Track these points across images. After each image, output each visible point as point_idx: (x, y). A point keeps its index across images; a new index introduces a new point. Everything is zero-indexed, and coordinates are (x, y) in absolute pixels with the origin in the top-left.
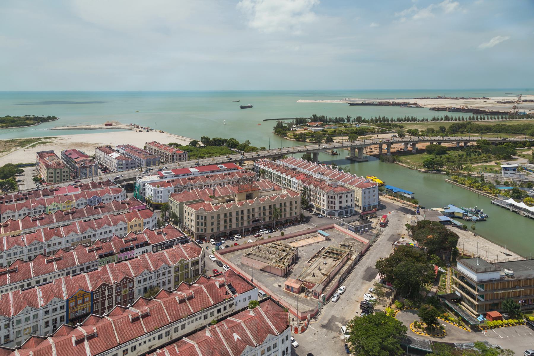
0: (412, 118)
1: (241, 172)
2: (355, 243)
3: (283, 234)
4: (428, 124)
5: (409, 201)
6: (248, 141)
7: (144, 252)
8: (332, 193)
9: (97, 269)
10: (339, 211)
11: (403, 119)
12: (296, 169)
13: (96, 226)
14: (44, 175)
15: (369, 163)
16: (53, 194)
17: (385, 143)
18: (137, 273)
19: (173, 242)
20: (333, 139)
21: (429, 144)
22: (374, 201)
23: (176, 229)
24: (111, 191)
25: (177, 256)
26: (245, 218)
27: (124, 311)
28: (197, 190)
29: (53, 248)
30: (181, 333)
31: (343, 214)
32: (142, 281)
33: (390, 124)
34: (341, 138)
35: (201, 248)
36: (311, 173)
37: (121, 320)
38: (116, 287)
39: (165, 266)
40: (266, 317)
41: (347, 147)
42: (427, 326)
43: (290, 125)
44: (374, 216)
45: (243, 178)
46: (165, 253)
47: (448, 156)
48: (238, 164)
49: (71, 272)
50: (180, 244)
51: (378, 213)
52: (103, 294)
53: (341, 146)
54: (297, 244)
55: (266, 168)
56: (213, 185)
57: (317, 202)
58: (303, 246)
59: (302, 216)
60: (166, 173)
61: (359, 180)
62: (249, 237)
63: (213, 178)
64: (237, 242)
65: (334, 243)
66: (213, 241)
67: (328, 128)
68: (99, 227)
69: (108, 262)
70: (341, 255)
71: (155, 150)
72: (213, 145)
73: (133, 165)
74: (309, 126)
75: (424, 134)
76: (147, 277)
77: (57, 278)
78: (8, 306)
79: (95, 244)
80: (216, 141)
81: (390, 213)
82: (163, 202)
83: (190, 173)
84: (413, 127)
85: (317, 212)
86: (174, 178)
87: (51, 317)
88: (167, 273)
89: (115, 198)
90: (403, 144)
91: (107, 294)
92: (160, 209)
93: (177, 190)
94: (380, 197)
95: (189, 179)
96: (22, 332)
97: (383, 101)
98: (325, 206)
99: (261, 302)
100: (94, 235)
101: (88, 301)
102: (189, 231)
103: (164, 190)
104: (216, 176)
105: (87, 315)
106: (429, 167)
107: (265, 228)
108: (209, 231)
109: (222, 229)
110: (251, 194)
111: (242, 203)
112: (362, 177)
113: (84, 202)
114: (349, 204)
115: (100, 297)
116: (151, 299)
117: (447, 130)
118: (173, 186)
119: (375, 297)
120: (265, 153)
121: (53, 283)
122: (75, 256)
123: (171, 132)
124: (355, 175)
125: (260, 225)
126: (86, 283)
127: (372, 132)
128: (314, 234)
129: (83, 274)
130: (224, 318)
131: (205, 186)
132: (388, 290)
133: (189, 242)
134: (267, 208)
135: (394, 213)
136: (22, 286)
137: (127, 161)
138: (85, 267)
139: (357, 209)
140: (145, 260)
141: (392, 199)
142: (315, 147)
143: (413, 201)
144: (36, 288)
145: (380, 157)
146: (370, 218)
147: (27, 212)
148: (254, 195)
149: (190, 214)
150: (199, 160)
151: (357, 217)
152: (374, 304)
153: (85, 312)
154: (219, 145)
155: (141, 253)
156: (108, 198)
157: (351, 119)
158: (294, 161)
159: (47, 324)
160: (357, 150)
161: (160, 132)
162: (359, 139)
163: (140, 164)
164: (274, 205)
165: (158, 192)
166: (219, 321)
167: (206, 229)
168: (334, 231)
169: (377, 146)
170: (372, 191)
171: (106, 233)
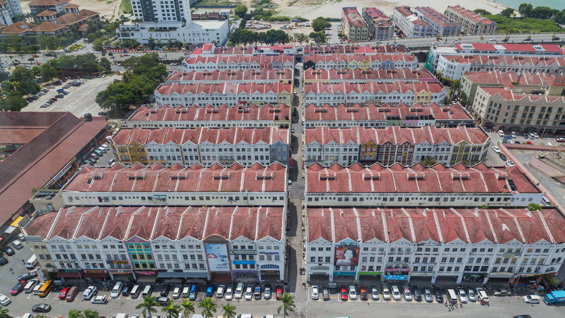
7: (427, 125)
9: (384, 128)
13: (387, 89)
16: (354, 52)
18: (418, 141)
19: (458, 122)
23: (464, 110)
25: (459, 137)
27: (403, 169)
28: (498, 73)
29: (351, 101)
32: (421, 150)
35: (488, 136)
37: (400, 175)
38: (399, 147)
39: (446, 143)
46: (448, 131)
49: (364, 125)
50: (465, 127)
52: (387, 150)
56: (520, 70)
60: (465, 47)
63: (523, 61)
66: (502, 133)
68: (390, 91)
69: (394, 125)
73: (429, 33)
76: (427, 147)
77: (353, 126)
78: (321, 136)
79: (385, 106)
82: (454, 79)
83: (495, 51)
87: (348, 154)
88: (445, 150)
89: (406, 65)
91: (390, 151)
92: (450, 86)
93: (473, 69)
95: (491, 58)
96: (329, 157)
100: (384, 98)
103: (459, 66)
104: (528, 60)
105: (373, 162)
111: (554, 99)
113: (378, 64)
116: (428, 168)
118: (470, 63)
121: (351, 129)
126: (375, 136)
129: (373, 129)
131: (509, 69)
133: (475, 127)
136: (329, 125)
138: (375, 123)
140: (427, 132)
144: (339, 129)
147: (333, 65)
149: (482, 98)
150: (510, 36)
153: (371, 159)
155: (424, 125)
156: (401, 64)
159: (345, 158)
163: (438, 32)
171: (394, 98)
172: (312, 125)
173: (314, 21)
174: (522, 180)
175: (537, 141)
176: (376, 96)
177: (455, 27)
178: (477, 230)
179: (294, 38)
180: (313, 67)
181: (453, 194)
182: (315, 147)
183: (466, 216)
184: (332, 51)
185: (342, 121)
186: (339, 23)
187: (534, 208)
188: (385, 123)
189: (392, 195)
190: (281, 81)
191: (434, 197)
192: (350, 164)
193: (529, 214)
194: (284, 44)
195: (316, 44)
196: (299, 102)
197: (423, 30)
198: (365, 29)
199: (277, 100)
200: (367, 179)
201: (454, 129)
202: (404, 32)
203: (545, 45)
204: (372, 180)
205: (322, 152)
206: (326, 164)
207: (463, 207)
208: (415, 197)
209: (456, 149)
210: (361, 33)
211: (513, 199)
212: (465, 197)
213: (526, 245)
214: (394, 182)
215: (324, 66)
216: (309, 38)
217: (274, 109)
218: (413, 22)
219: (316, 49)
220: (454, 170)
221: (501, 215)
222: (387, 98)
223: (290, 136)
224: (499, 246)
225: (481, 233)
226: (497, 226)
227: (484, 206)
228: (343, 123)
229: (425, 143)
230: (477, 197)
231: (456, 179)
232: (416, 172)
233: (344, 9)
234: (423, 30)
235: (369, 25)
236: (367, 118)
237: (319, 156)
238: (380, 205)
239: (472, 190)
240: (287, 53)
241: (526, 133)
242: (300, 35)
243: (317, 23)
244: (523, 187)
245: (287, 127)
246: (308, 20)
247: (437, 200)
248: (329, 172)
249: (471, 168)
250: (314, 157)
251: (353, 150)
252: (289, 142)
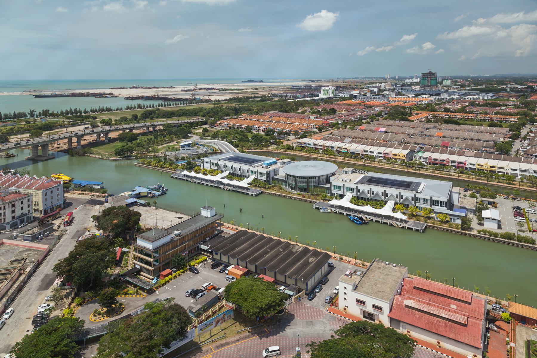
0: (106, 108)
2: (31, 253)
4: (122, 113)
5: (98, 192)
10: (11, 223)
11: (98, 109)
15: (57, 160)
20: (8, 139)
21: (121, 132)
22: (58, 200)
31: (17, 225)
33: (83, 116)
34: (19, 136)
44: (57, 216)
47: (138, 141)
51: (62, 212)
70: (9, 274)
75: (118, 122)
81: (76, 209)
84: (106, 117)
90: (96, 135)
94: (66, 195)
106: (120, 155)
112: (44, 177)
114: (25, 211)
117: (139, 118)
124: (35, 176)
127: (62, 126)
135: (81, 208)
141: (80, 194)
143: (102, 191)
145: (70, 152)
146: (52, 221)
151: (36, 223)
160: (40, 148)
162: (44, 134)
169: (66, 140)
170: (55, 190)
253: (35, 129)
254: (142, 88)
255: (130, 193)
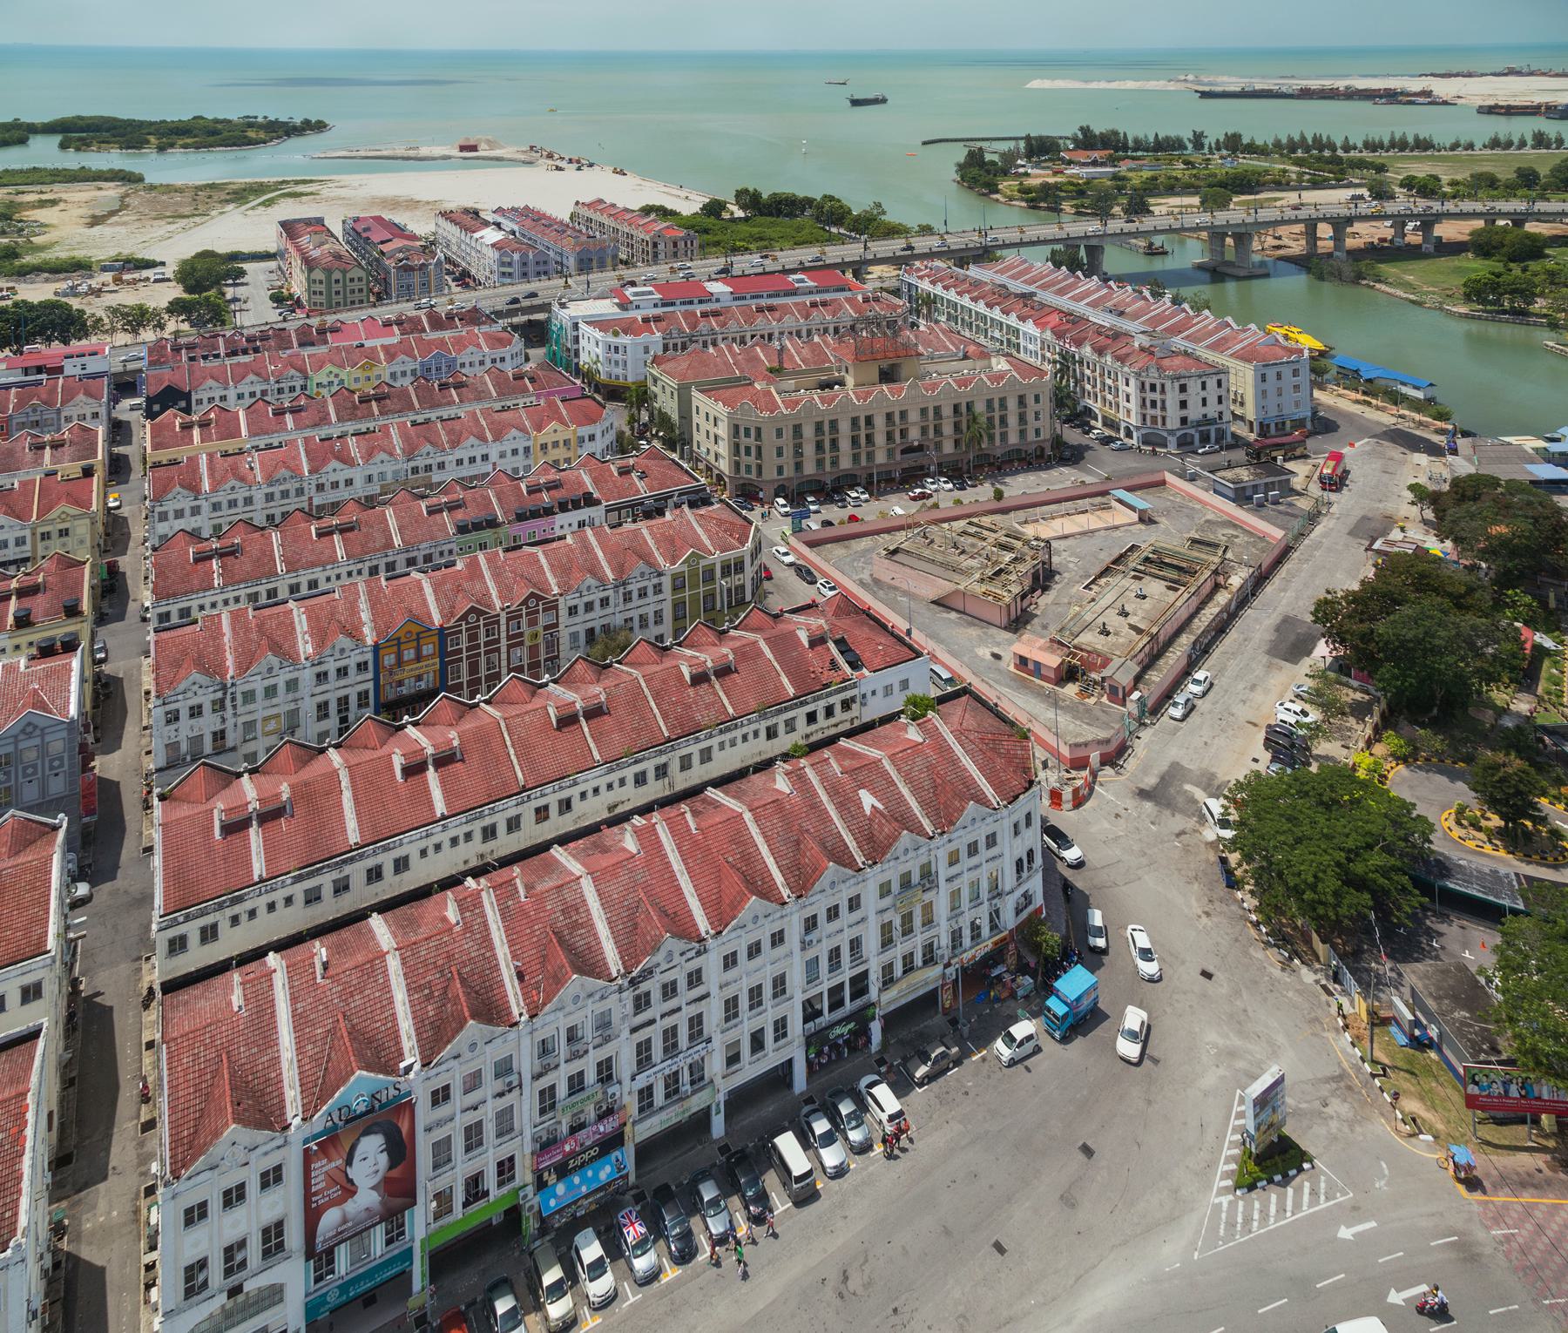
1: (860, 298)
3: (999, 495)
5: (1418, 410)
6: (879, 205)
7: (581, 524)
8: (1153, 377)
9: (453, 564)
10: (1179, 433)
11: (1386, 142)
12: (1033, 294)
13: (444, 438)
14: (298, 286)
16: (326, 342)
17: (1325, 219)
18: (566, 583)
19: (666, 499)
22: (1297, 404)
24: (481, 341)
25: (678, 543)
26: (880, 439)
27: (533, 694)
28: (730, 349)
29: (331, 496)
30: (698, 773)
31: (1192, 443)
32: (581, 609)
34: (1175, 201)
35: (751, 523)
36: (1081, 308)
37: (527, 718)
38: (509, 620)
39: (647, 570)
40: (958, 750)
41: (1198, 228)
42: (1502, 823)
43: (1009, 158)
44: (1298, 452)
45: (867, 318)
46: (645, 532)
47: (1550, 264)
48: (849, 275)
49: (382, 568)
50: (685, 507)
51: (1311, 443)
52: (473, 637)
53: (1177, 225)
54: (1047, 530)
55: (938, 290)
57: (1104, 399)
58: (1065, 537)
59: (1058, 442)
60: (636, 294)
61: (1242, 336)
62: (893, 498)
63: (777, 315)
64: (857, 512)
65: (1167, 532)
67: (1130, 170)
68: (455, 444)
69: (483, 547)
70: (1193, 573)
71: (602, 225)
72: (771, 214)
74: (1070, 163)
75: (1461, 191)
76: (596, 597)
77: (345, 581)
78: (219, 650)
79: (444, 492)
80: (780, 202)
81: (1352, 445)
82: (630, 379)
83: (708, 298)
84: (1421, 170)
85: (1108, 432)
86: (659, 311)
87: (333, 691)
88: (650, 591)
89: (494, 361)
90: (1388, 223)
91: (482, 639)
92: (623, 400)
94: (1317, 393)
95: (705, 315)
96: (259, 725)
97: (1314, 84)
98: (1133, 414)
99: (942, 700)
100: (441, 466)
101: (432, 656)
102: (709, 469)
104: (785, 309)
105: (432, 694)
106: (1484, 302)
107: (941, 474)
108: (770, 474)
109: (809, 469)
110: (894, 367)
111: (869, 394)
112: (1253, 326)
113: (409, 367)
114: (1212, 410)
115: (464, 646)
116: (610, 666)
119: (1314, 716)
120: (933, 243)
121: (337, 596)
122: (392, 523)
123: (649, 172)
124: (1229, 319)
125: (925, 462)
126: (425, 601)
127: (1281, 184)
128: (1098, 500)
129: (415, 575)
130: (831, 741)
132: (1358, 696)
134: (947, 411)
135: (1368, 448)
136: (253, 597)
137: (524, 255)
138: (420, 556)
139: (1240, 429)
141: (1357, 402)
142: (1092, 226)
143: (1433, 411)
144: (291, 604)
145: (1307, 263)
147: (258, 389)
148: (904, 372)
151: (1239, 455)
152: (1310, 738)
153: (423, 685)
154: (791, 215)
156: (476, 359)
157: (1206, 142)
158: (1027, 271)
160: (1229, 241)
161: (615, 171)
164: (969, 406)
165: (616, 348)
166: (814, 747)
167: (759, 467)
168: (1165, 495)
169: (1299, 228)
170: (1287, 372)
171: (472, 460)
172: (185, 613)
173: (184, 263)
174: (866, 629)
175: (871, 510)
176: (412, 464)
177: (603, 249)
178: (798, 843)
179: (106, 321)
180: (183, 404)
181: (701, 735)
182: (195, 701)
183: (756, 804)
184: (252, 345)
185: (302, 572)
186: (272, 265)
187: (918, 709)
188: (453, 546)
189: (509, 808)
190: (51, 474)
191: (649, 766)
192: (347, 728)
193: (913, 734)
194: (66, 342)
195: (194, 331)
196: (129, 535)
197: (525, 264)
198: (356, 273)
199: (28, 547)
200: (414, 770)
201: (658, 521)
202: (473, 272)
203: (812, 273)
204: (431, 768)
205: (230, 711)
206: (250, 758)
207: (741, 774)
208: (588, 787)
209: (678, 583)
210: (345, 286)
211: (864, 696)
212: (738, 733)
213: (938, 841)
214: (512, 752)
215: (223, 398)
216: (166, 317)
217: (14, 584)
218: (493, 245)
219: (190, 347)
220: (688, 652)
221: (847, 763)
222: (450, 467)
223: (83, 680)
224: (875, 876)
225: (812, 847)
226: (848, 805)
227: (796, 747)
228: (304, 579)
229: (587, 583)
230: (769, 723)
231: (699, 679)
232: (576, 690)
233: (284, 224)
234: (525, 264)
235: (369, 263)
236: (389, 544)
237: (215, 734)
238: (474, 863)
239: (753, 705)
240: (78, 371)
241: (838, 493)
242: (132, 308)
243: (194, 269)
244: (876, 652)
245: (70, 646)
246: (163, 264)
247: (662, 771)
248: (258, 788)
249: (733, 633)
250: (197, 741)
251: (352, 671)
252: (81, 704)
253: (1210, 186)
254: (1544, 74)
255: (1541, 444)
